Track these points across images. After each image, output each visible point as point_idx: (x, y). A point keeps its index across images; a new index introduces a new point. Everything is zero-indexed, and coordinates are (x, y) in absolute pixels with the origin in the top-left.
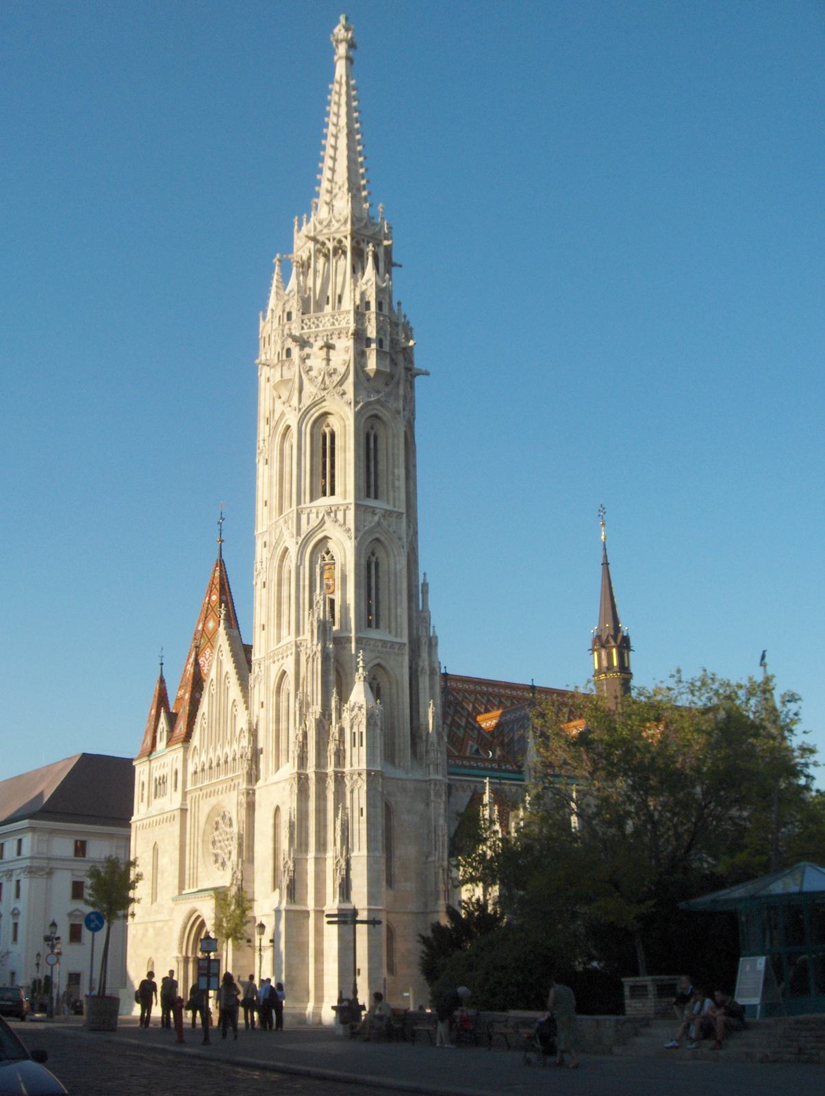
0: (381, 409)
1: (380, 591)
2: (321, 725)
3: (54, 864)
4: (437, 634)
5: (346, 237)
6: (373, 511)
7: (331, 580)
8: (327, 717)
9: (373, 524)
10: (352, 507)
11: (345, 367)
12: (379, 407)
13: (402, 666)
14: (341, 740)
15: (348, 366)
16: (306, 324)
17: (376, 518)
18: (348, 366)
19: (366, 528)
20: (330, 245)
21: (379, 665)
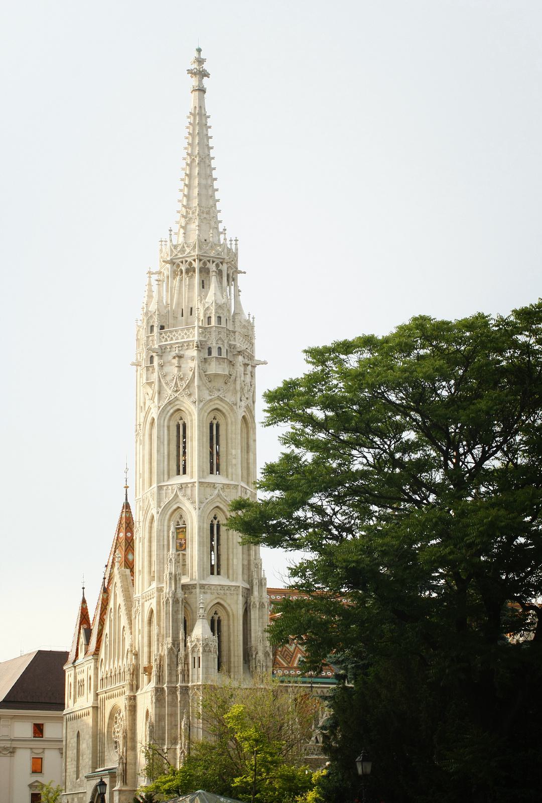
0: (221, 403)
1: (221, 546)
2: (171, 652)
3: (15, 744)
4: (266, 576)
5: (194, 260)
6: (213, 486)
7: (183, 540)
8: (176, 646)
9: (213, 497)
10: (196, 485)
11: (191, 373)
12: (218, 402)
13: (237, 604)
14: (186, 663)
15: (194, 373)
16: (163, 337)
17: (216, 492)
18: (194, 373)
19: (208, 500)
20: (183, 267)
21: (218, 603)
